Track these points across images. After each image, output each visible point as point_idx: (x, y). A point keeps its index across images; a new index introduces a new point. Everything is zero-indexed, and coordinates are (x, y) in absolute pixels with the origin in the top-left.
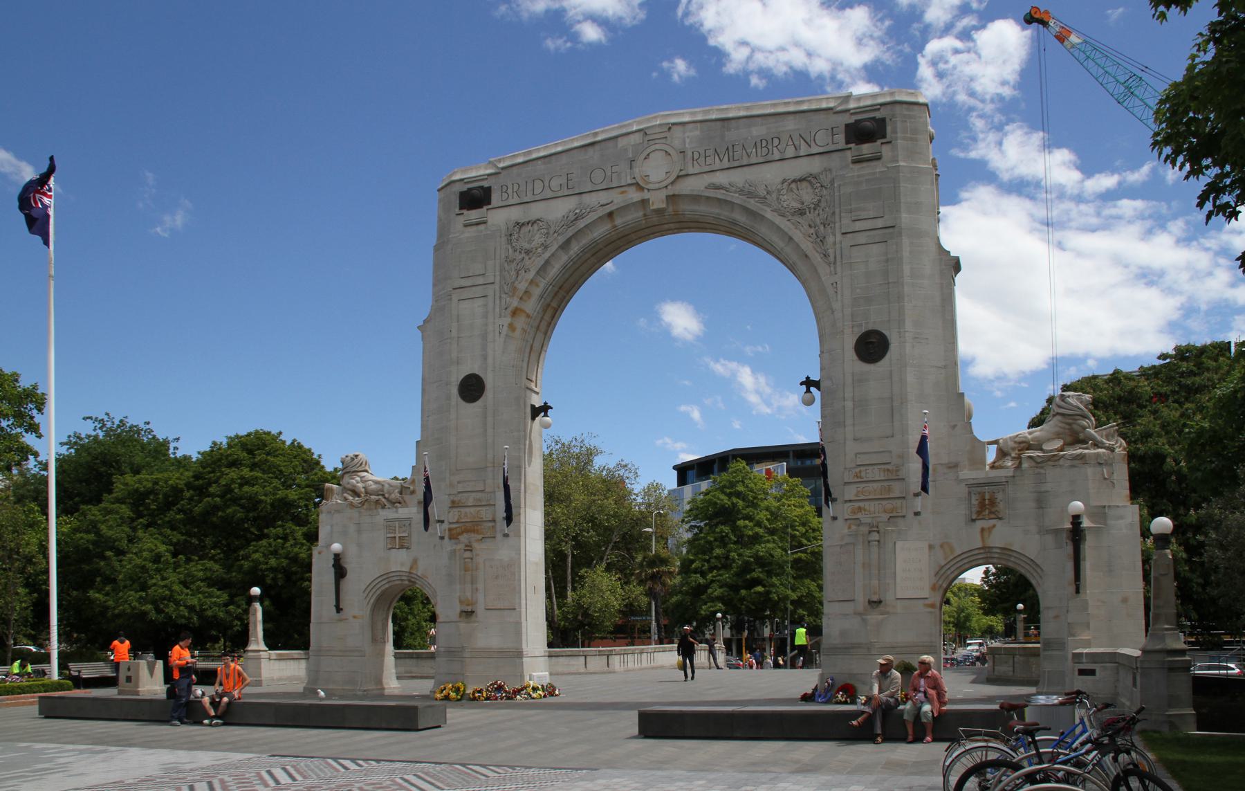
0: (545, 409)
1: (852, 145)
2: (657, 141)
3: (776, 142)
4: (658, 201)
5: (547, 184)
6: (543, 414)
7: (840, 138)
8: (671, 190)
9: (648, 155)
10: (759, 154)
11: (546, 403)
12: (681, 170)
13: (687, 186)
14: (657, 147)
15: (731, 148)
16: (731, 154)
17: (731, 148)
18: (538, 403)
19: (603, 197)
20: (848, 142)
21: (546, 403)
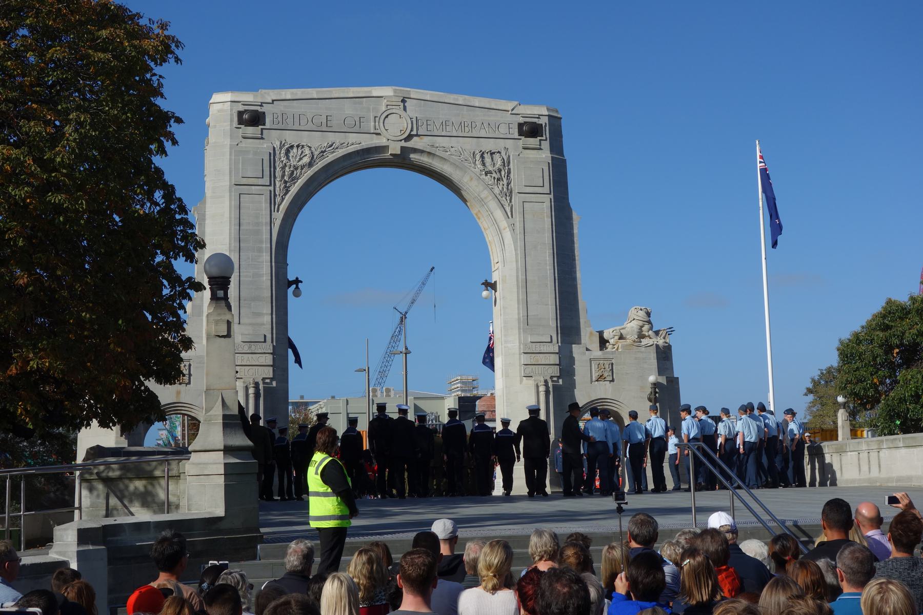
0: (297, 282)
1: (523, 138)
2: (394, 107)
3: (474, 125)
4: (395, 149)
5: (310, 120)
6: (294, 286)
7: (515, 133)
8: (403, 144)
9: (388, 115)
10: (463, 131)
11: (297, 278)
12: (412, 130)
13: (415, 143)
14: (394, 111)
15: (444, 123)
16: (444, 127)
17: (444, 123)
18: (291, 278)
19: (352, 138)
20: (520, 135)
21: (297, 278)
